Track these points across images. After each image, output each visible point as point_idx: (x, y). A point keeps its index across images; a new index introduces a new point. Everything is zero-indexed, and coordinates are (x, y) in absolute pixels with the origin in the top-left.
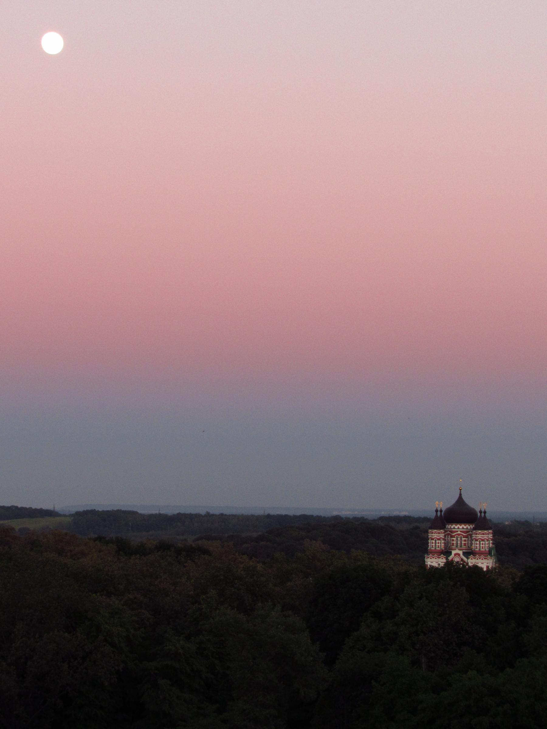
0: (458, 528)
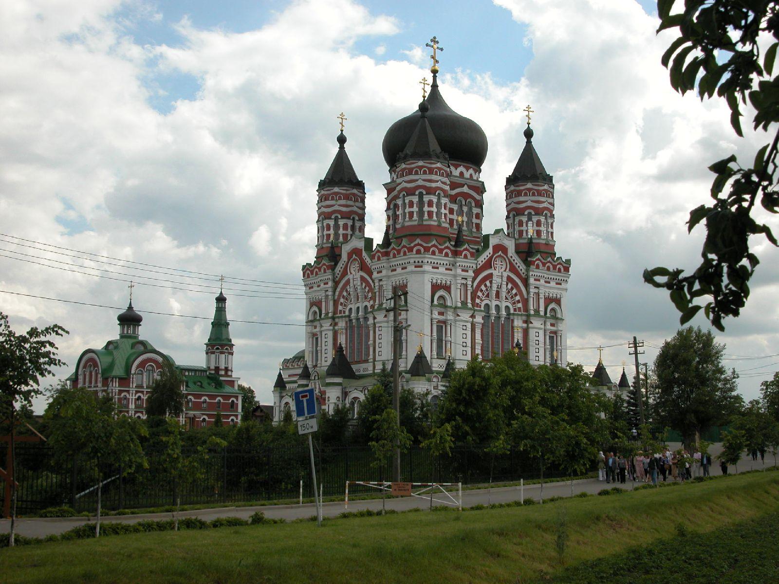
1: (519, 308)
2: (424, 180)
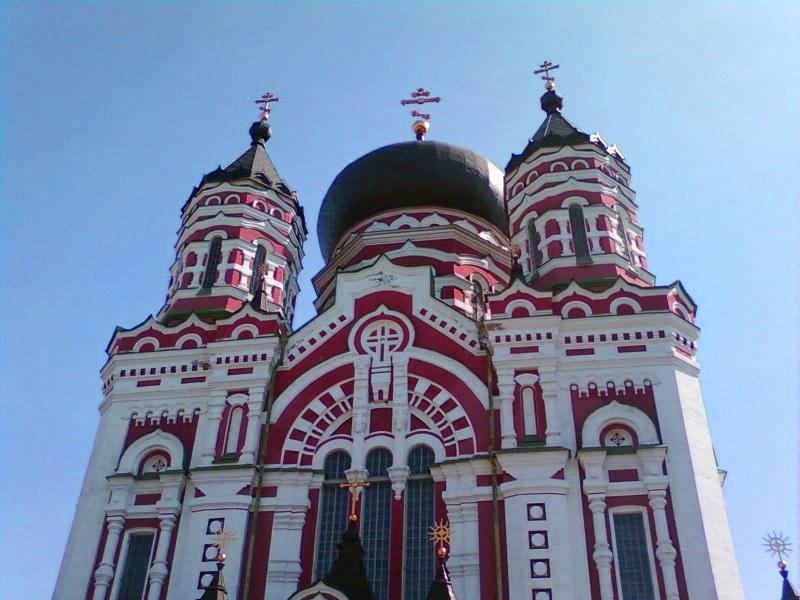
1: (466, 445)
2: (226, 215)
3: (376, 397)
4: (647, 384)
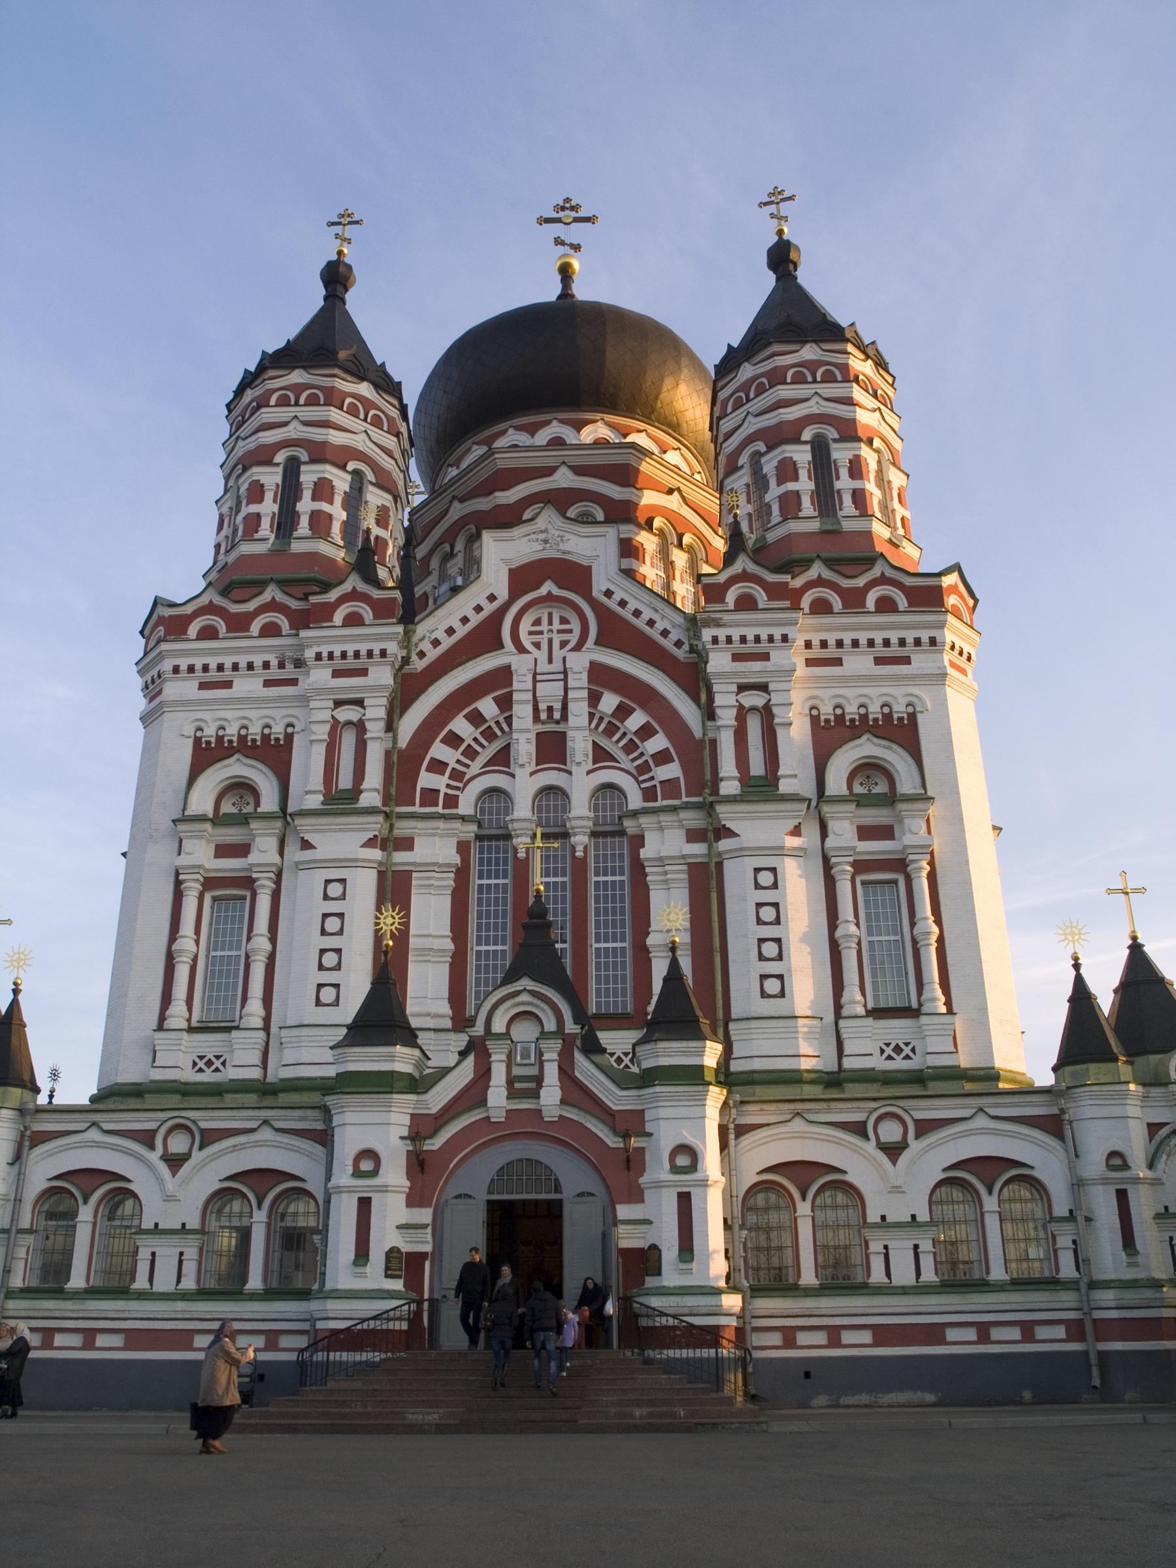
0: (557, 442)
1: (670, 787)
2: (307, 424)
3: (544, 716)
4: (910, 710)
